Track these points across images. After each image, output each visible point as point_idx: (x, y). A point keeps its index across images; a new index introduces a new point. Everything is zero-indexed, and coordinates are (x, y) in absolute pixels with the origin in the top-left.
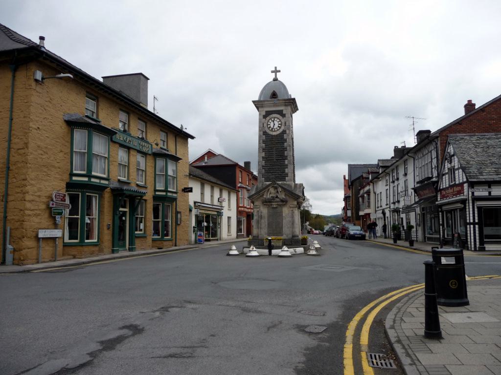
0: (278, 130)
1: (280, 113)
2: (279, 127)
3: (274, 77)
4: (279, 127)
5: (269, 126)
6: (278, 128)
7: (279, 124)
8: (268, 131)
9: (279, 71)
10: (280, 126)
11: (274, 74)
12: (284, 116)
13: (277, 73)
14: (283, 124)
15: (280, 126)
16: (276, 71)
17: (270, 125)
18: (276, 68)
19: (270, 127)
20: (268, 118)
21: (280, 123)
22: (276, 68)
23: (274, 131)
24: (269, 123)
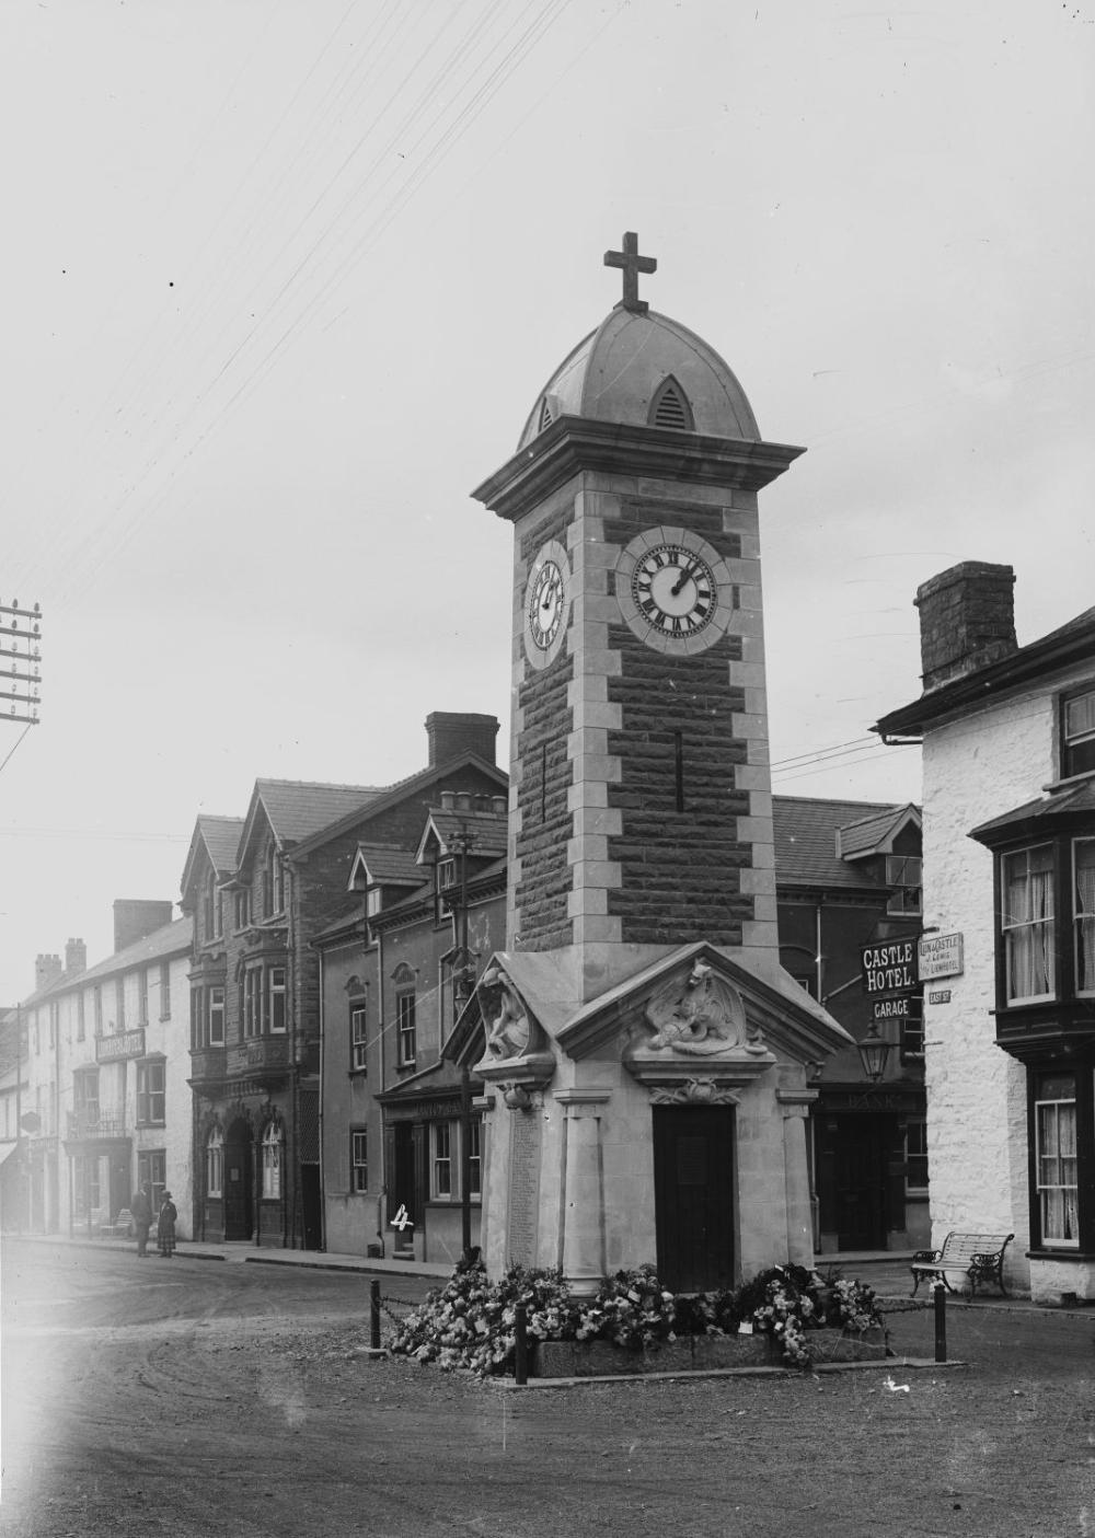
0: (702, 625)
1: (705, 523)
2: (699, 609)
3: (619, 296)
4: (699, 609)
5: (644, 597)
6: (697, 618)
7: (703, 594)
8: (639, 628)
9: (650, 266)
10: (705, 603)
11: (619, 272)
12: (729, 547)
13: (641, 276)
14: (725, 596)
15: (705, 603)
16: (630, 261)
17: (647, 588)
18: (631, 240)
19: (650, 605)
20: (638, 546)
21: (704, 585)
22: (631, 240)
23: (676, 633)
24: (644, 579)
